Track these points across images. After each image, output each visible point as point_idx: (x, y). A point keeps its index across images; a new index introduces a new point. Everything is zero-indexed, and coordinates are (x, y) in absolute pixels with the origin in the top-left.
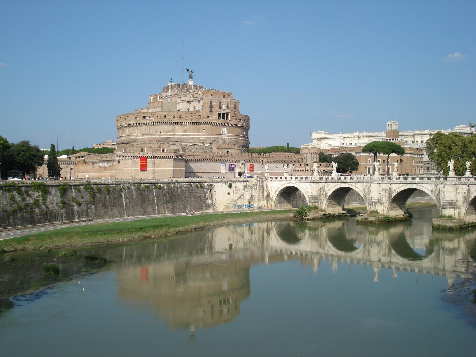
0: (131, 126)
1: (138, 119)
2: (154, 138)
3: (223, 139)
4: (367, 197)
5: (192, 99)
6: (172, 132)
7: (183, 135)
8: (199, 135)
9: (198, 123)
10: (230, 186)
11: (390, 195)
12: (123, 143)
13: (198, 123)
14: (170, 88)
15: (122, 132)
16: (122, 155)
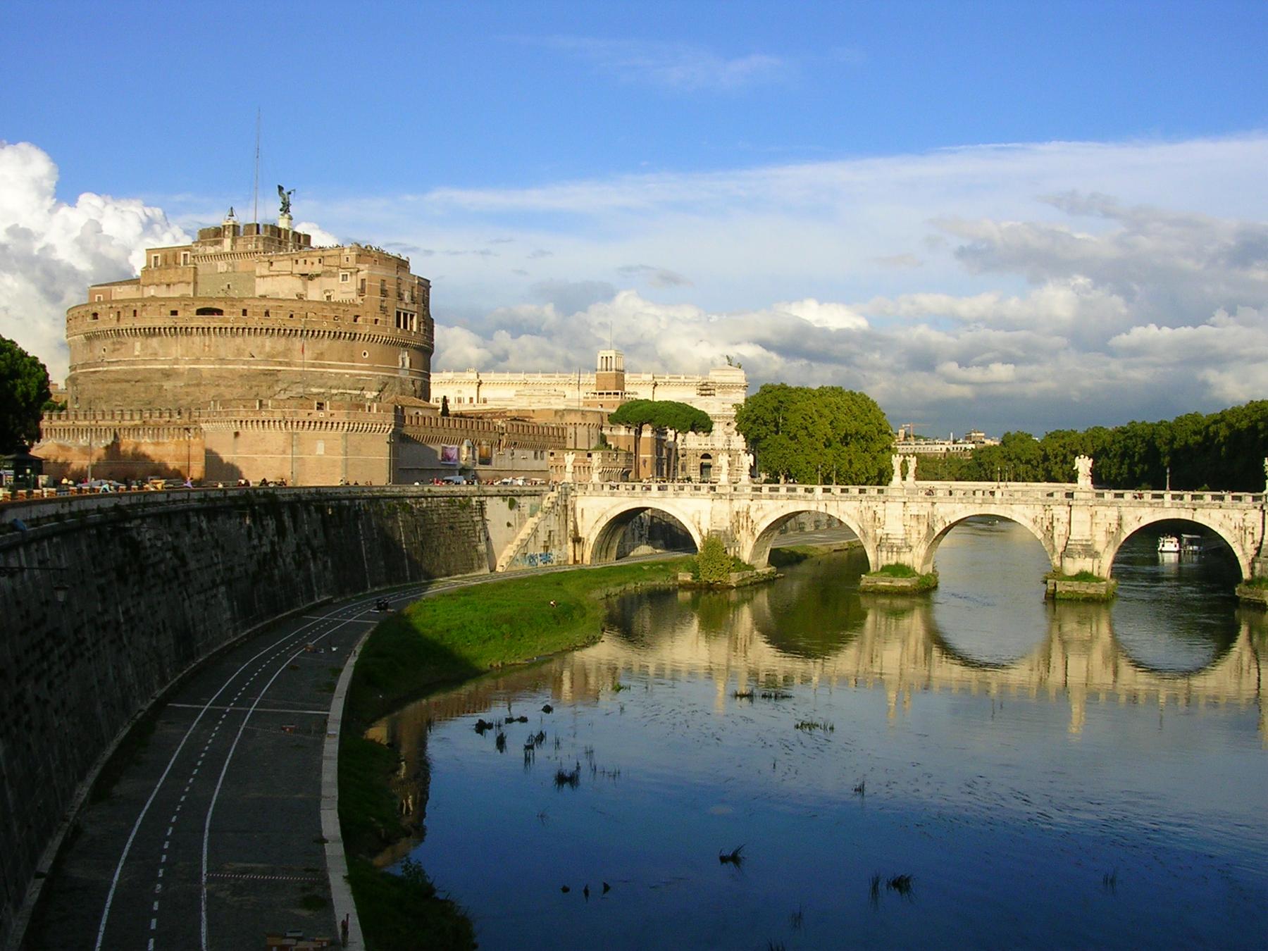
0: (152, 332)
1: (180, 314)
2: (231, 371)
3: (402, 382)
4: (871, 534)
5: (317, 268)
6: (286, 356)
7: (313, 366)
8: (353, 368)
9: (353, 337)
10: (512, 505)
11: (930, 528)
12: (117, 381)
13: (353, 337)
14: (229, 233)
15: (114, 351)
16: (252, 417)
